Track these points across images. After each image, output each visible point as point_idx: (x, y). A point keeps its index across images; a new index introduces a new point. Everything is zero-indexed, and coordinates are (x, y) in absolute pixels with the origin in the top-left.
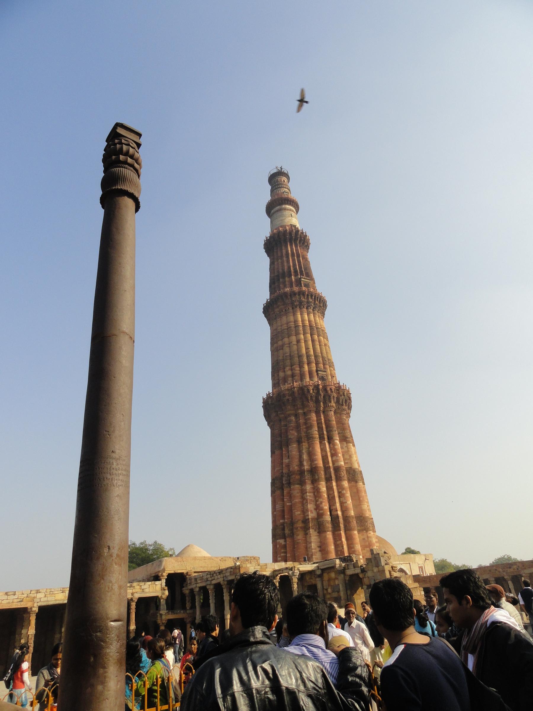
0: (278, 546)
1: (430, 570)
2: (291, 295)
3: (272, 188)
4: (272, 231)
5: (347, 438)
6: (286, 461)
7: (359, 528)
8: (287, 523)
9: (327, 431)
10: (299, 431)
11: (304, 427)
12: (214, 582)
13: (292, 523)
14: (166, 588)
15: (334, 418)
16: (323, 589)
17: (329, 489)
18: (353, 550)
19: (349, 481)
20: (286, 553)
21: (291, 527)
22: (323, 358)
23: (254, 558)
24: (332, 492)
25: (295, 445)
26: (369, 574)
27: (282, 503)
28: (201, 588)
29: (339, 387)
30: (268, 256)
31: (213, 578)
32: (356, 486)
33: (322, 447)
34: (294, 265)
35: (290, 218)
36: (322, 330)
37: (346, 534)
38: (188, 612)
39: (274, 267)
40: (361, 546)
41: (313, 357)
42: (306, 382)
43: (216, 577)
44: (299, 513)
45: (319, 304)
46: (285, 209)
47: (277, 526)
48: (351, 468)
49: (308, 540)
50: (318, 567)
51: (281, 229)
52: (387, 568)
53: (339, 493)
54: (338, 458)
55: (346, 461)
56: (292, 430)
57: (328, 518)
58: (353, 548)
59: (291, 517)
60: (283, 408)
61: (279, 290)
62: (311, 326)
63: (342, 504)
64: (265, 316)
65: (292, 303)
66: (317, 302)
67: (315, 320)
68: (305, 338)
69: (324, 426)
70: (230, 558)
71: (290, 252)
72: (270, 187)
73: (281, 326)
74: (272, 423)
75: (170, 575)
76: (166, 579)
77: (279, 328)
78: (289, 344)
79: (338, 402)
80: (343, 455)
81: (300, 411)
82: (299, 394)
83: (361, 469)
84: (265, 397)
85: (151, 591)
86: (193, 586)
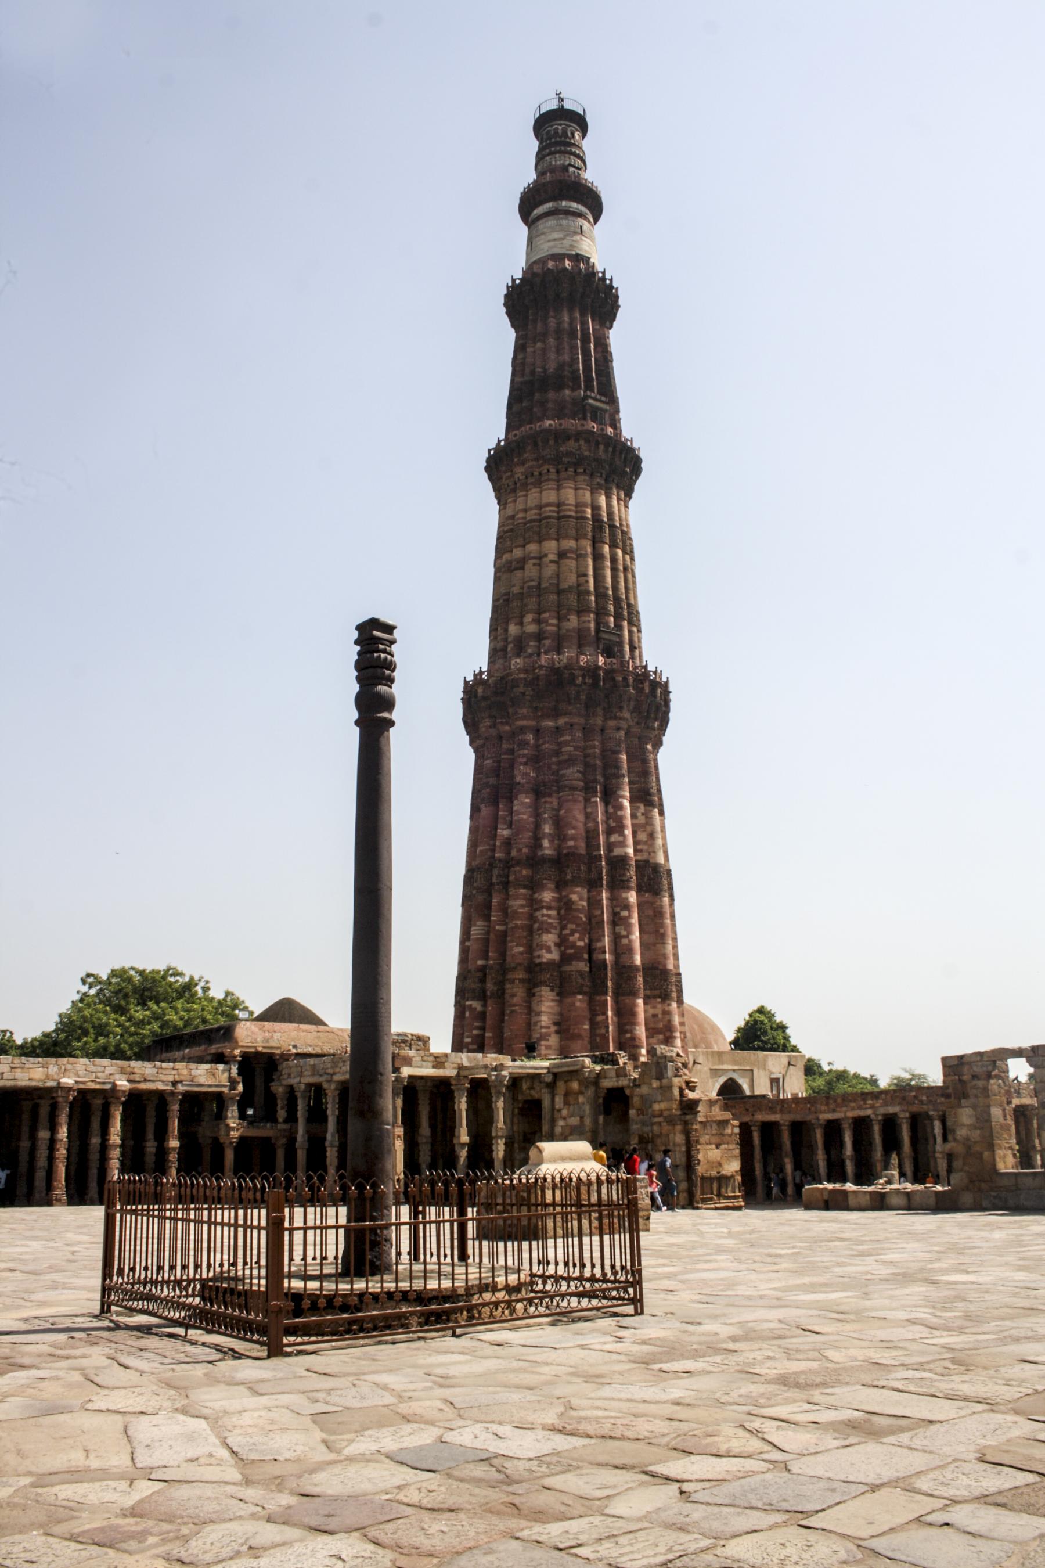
0: (467, 1014)
1: (796, 1086)
2: (556, 441)
6: (504, 832)
7: (648, 992)
8: (491, 967)
9: (604, 775)
10: (537, 770)
11: (554, 759)
12: (337, 1078)
13: (503, 969)
14: (239, 1079)
18: (628, 1035)
19: (639, 890)
20: (483, 1029)
22: (617, 600)
23: (419, 1038)
25: (528, 800)
26: (644, 1090)
28: (309, 1085)
29: (646, 674)
30: (512, 326)
31: (337, 1070)
32: (652, 903)
33: (589, 810)
37: (616, 1001)
38: (280, 1126)
39: (524, 358)
41: (593, 598)
44: (521, 949)
47: (469, 971)
49: (534, 1006)
51: (551, 264)
52: (676, 1081)
54: (621, 839)
55: (639, 847)
56: (526, 764)
57: (583, 966)
58: (631, 1032)
59: (503, 954)
60: (511, 710)
61: (530, 422)
63: (616, 938)
64: (490, 478)
67: (609, 505)
69: (598, 762)
71: (566, 326)
72: (534, 145)
74: (479, 742)
75: (245, 1056)
76: (240, 1063)
78: (540, 558)
79: (637, 709)
80: (634, 833)
83: (673, 866)
84: (470, 678)
85: (210, 1083)
86: (294, 1081)
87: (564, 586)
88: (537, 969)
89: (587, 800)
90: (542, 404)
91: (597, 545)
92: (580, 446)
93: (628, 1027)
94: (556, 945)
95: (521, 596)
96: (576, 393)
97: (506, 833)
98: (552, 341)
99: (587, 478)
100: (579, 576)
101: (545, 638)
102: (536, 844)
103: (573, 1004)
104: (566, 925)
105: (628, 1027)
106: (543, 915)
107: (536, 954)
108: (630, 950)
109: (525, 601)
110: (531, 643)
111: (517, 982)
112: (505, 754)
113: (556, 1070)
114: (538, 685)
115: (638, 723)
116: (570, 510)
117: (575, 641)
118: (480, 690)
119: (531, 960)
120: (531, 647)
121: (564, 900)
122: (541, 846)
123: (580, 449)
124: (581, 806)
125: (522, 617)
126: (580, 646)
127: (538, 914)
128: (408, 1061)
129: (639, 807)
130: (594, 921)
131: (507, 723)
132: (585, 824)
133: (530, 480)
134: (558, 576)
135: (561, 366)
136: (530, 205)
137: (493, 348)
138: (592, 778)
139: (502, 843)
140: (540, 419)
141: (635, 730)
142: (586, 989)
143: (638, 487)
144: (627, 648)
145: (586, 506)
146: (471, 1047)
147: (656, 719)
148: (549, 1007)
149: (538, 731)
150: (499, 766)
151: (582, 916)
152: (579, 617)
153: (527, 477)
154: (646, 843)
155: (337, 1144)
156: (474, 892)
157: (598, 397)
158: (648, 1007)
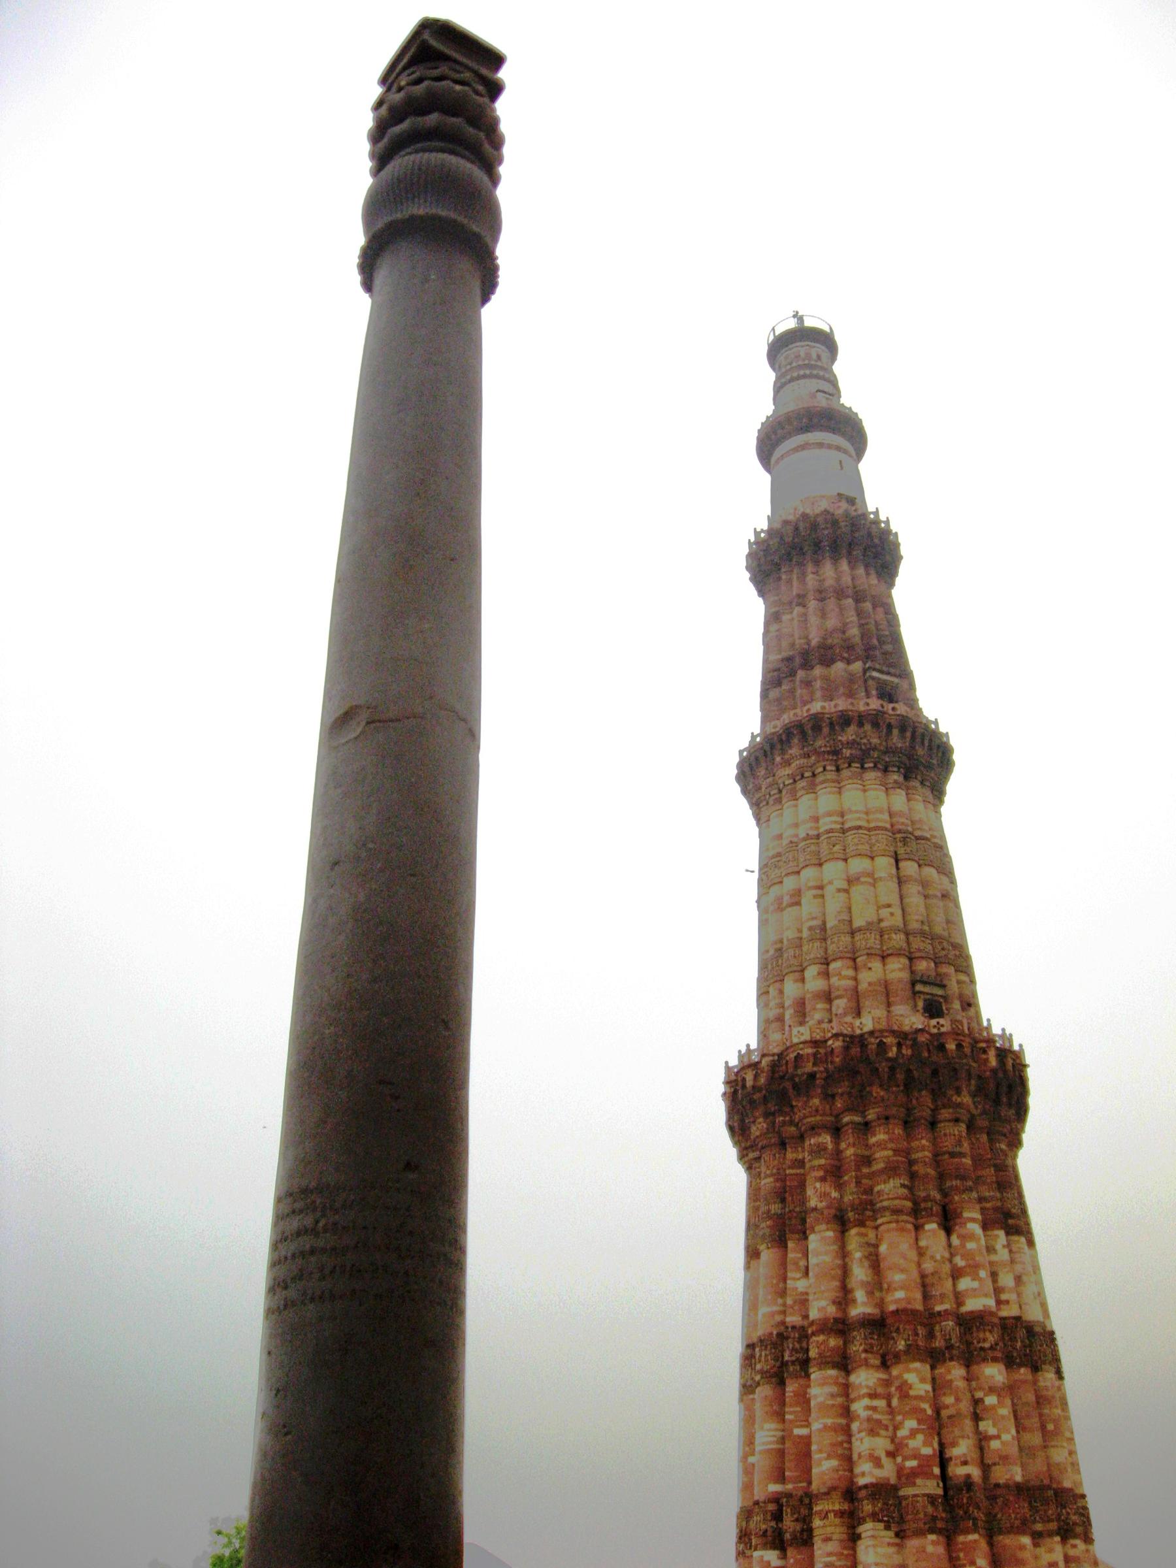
2: (832, 725)
3: (778, 379)
5: (1008, 1215)
6: (798, 1284)
8: (789, 1495)
10: (840, 1187)
15: (966, 1145)
21: (804, 1511)
24: (949, 1400)
27: (773, 1426)
29: (990, 1041)
30: (761, 593)
32: (1035, 1382)
33: (922, 1243)
36: (940, 848)
37: (991, 1544)
44: (834, 1463)
46: (820, 445)
47: (757, 1503)
55: (1004, 1297)
56: (823, 1179)
57: (932, 1487)
63: (982, 1441)
64: (745, 792)
65: (836, 753)
72: (771, 376)
73: (796, 825)
74: (752, 1155)
78: (821, 887)
79: (979, 1092)
80: (994, 1275)
84: (734, 1062)
87: (858, 922)
88: (863, 1493)
89: (918, 1228)
91: (901, 864)
92: (865, 732)
94: (891, 1455)
95: (798, 943)
97: (801, 1285)
98: (812, 604)
99: (879, 774)
100: (879, 908)
101: (838, 997)
102: (844, 1297)
103: (923, 1550)
104: (901, 1423)
106: (868, 1408)
107: (857, 1470)
108: (1005, 1459)
109: (805, 948)
110: (820, 1006)
111: (831, 1516)
112: (789, 1168)
115: (984, 1112)
116: (859, 819)
118: (749, 1077)
119: (851, 1481)
121: (897, 1383)
122: (854, 1301)
124: (912, 1241)
125: (803, 971)
126: (889, 1005)
129: (997, 1236)
130: (944, 1413)
131: (791, 1123)
132: (919, 1265)
133: (801, 784)
134: (850, 908)
136: (770, 444)
137: (739, 625)
138: (923, 1194)
139: (795, 1302)
140: (805, 703)
141: (983, 1122)
142: (940, 1525)
144: (957, 1005)
145: (881, 812)
147: (1010, 1105)
150: (784, 1188)
152: (884, 965)
153: (795, 781)
156: (758, 1378)
157: (885, 669)
158: (1041, 1551)
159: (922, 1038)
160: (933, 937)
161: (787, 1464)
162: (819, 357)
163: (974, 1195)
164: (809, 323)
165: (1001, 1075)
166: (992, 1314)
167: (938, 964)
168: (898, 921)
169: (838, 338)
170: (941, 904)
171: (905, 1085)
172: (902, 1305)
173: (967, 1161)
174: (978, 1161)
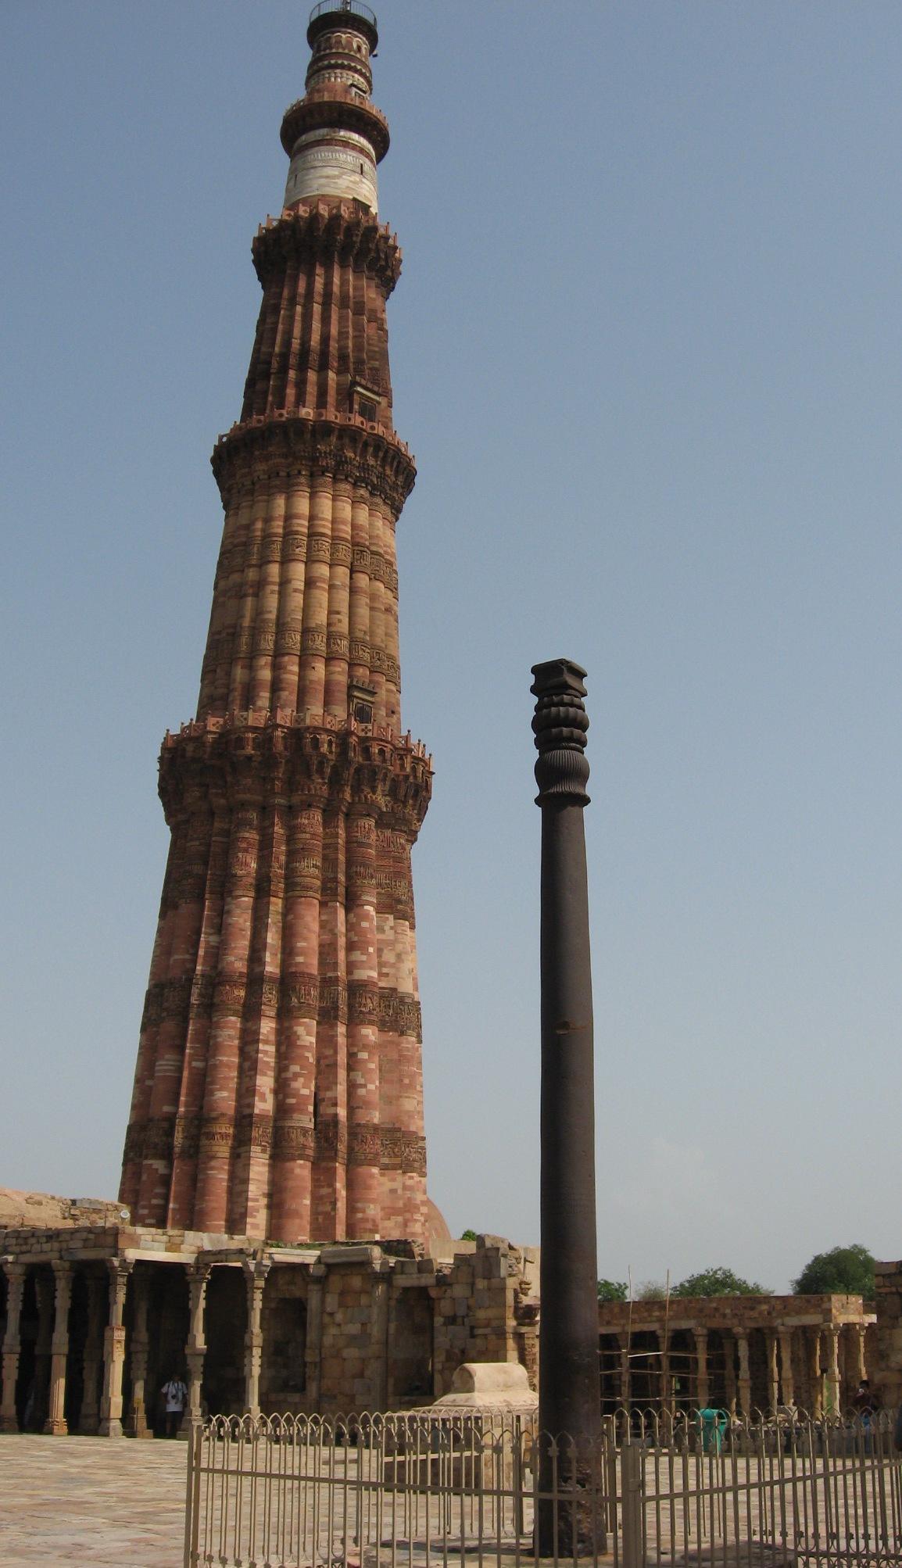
0: (144, 1177)
2: (314, 432)
4: (292, 206)
5: (399, 901)
13: (201, 1120)
15: (373, 836)
16: (323, 1311)
17: (326, 1040)
18: (360, 1215)
20: (166, 1198)
24: (329, 1052)
26: (459, 1291)
31: (24, 1248)
32: (398, 1044)
33: (324, 918)
34: (343, 335)
35: (357, 177)
36: (391, 564)
37: (347, 1172)
40: (383, 1209)
41: (345, 643)
42: (313, 716)
43: (37, 1247)
45: (389, 476)
46: (346, 144)
47: (151, 1120)
48: (394, 990)
50: (319, 1257)
51: (324, 210)
52: (512, 1283)
53: (351, 1056)
54: (364, 958)
55: (385, 970)
56: (246, 851)
58: (364, 1212)
60: (229, 779)
61: (281, 406)
62: (355, 544)
63: (352, 1087)
65: (314, 460)
66: (388, 472)
68: (331, 578)
69: (342, 858)
70: (53, 1198)
72: (307, 54)
74: (181, 817)
77: (259, 525)
79: (393, 793)
80: (380, 951)
81: (280, 801)
82: (286, 748)
84: (176, 730)
90: (301, 384)
93: (359, 1205)
96: (342, 378)
97: (214, 939)
99: (348, 487)
105: (359, 1205)
107: (247, 1101)
108: (367, 1104)
113: (331, 1261)
114: (270, 749)
116: (324, 526)
117: (321, 696)
118: (190, 748)
120: (264, 699)
123: (342, 449)
126: (327, 703)
127: (250, 1049)
128: (135, 1242)
135: (325, 339)
143: (410, 504)
144: (383, 712)
145: (344, 523)
146: (148, 1221)
148: (259, 1173)
149: (264, 808)
151: (309, 1055)
154: (393, 966)
155: (18, 1349)
157: (369, 385)
159: (353, 740)
160: (373, 647)
161: (183, 1091)
162: (359, 48)
163: (374, 881)
164: (355, 9)
165: (411, 779)
166: (375, 984)
167: (370, 668)
168: (344, 627)
169: (379, 30)
170: (383, 616)
171: (330, 779)
172: (299, 969)
173: (373, 852)
174: (383, 853)
